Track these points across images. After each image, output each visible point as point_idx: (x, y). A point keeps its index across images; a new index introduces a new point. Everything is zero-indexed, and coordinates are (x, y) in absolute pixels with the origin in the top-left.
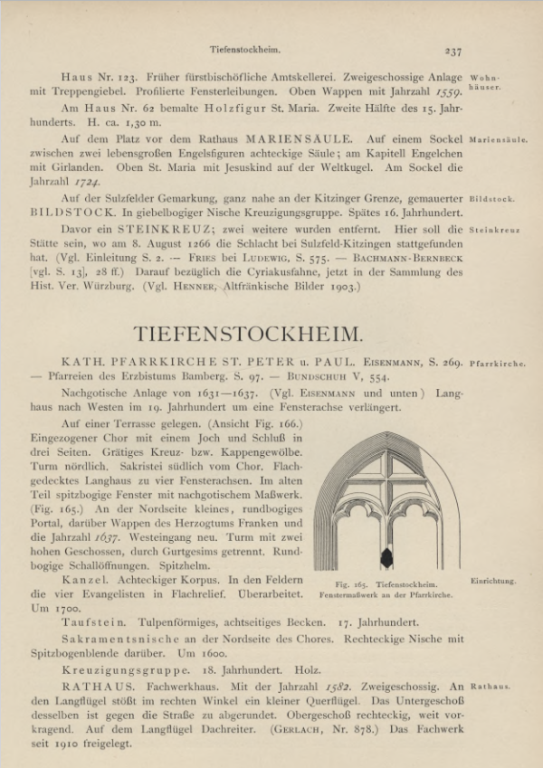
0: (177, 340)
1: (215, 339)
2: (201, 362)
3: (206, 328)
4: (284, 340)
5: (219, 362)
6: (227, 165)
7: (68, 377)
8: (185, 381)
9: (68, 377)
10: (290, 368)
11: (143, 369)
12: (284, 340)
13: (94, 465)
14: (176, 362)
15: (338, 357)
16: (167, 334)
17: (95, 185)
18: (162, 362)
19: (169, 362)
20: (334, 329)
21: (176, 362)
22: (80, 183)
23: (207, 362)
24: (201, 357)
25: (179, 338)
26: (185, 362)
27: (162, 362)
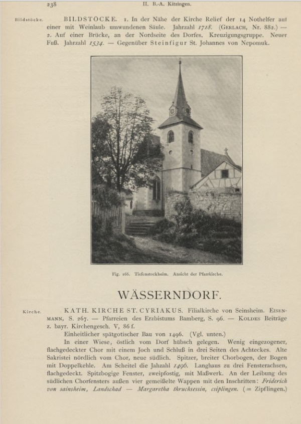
0: (213, 298)
1: (179, 298)
2: (115, 310)
3: (175, 292)
4: (165, 298)
5: (125, 310)
6: (201, 41)
7: (113, 319)
8: (181, 321)
9: (113, 319)
10: (104, 314)
11: (157, 315)
12: (165, 298)
13: (90, 357)
14: (101, 311)
15: (174, 308)
16: (160, 295)
17: (101, 45)
18: (167, 311)
19: (97, 310)
20: (183, 292)
21: (101, 311)
22: (201, 28)
23: (119, 311)
24: (115, 308)
25: (215, 298)
26: (106, 311)
27: (167, 311)
